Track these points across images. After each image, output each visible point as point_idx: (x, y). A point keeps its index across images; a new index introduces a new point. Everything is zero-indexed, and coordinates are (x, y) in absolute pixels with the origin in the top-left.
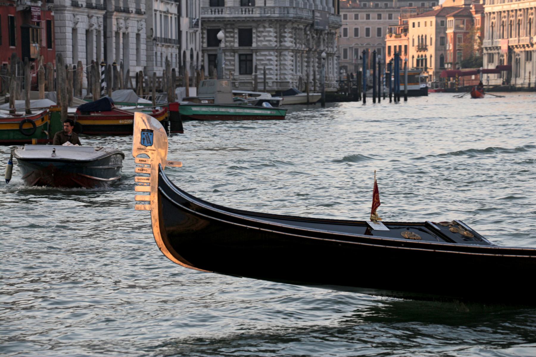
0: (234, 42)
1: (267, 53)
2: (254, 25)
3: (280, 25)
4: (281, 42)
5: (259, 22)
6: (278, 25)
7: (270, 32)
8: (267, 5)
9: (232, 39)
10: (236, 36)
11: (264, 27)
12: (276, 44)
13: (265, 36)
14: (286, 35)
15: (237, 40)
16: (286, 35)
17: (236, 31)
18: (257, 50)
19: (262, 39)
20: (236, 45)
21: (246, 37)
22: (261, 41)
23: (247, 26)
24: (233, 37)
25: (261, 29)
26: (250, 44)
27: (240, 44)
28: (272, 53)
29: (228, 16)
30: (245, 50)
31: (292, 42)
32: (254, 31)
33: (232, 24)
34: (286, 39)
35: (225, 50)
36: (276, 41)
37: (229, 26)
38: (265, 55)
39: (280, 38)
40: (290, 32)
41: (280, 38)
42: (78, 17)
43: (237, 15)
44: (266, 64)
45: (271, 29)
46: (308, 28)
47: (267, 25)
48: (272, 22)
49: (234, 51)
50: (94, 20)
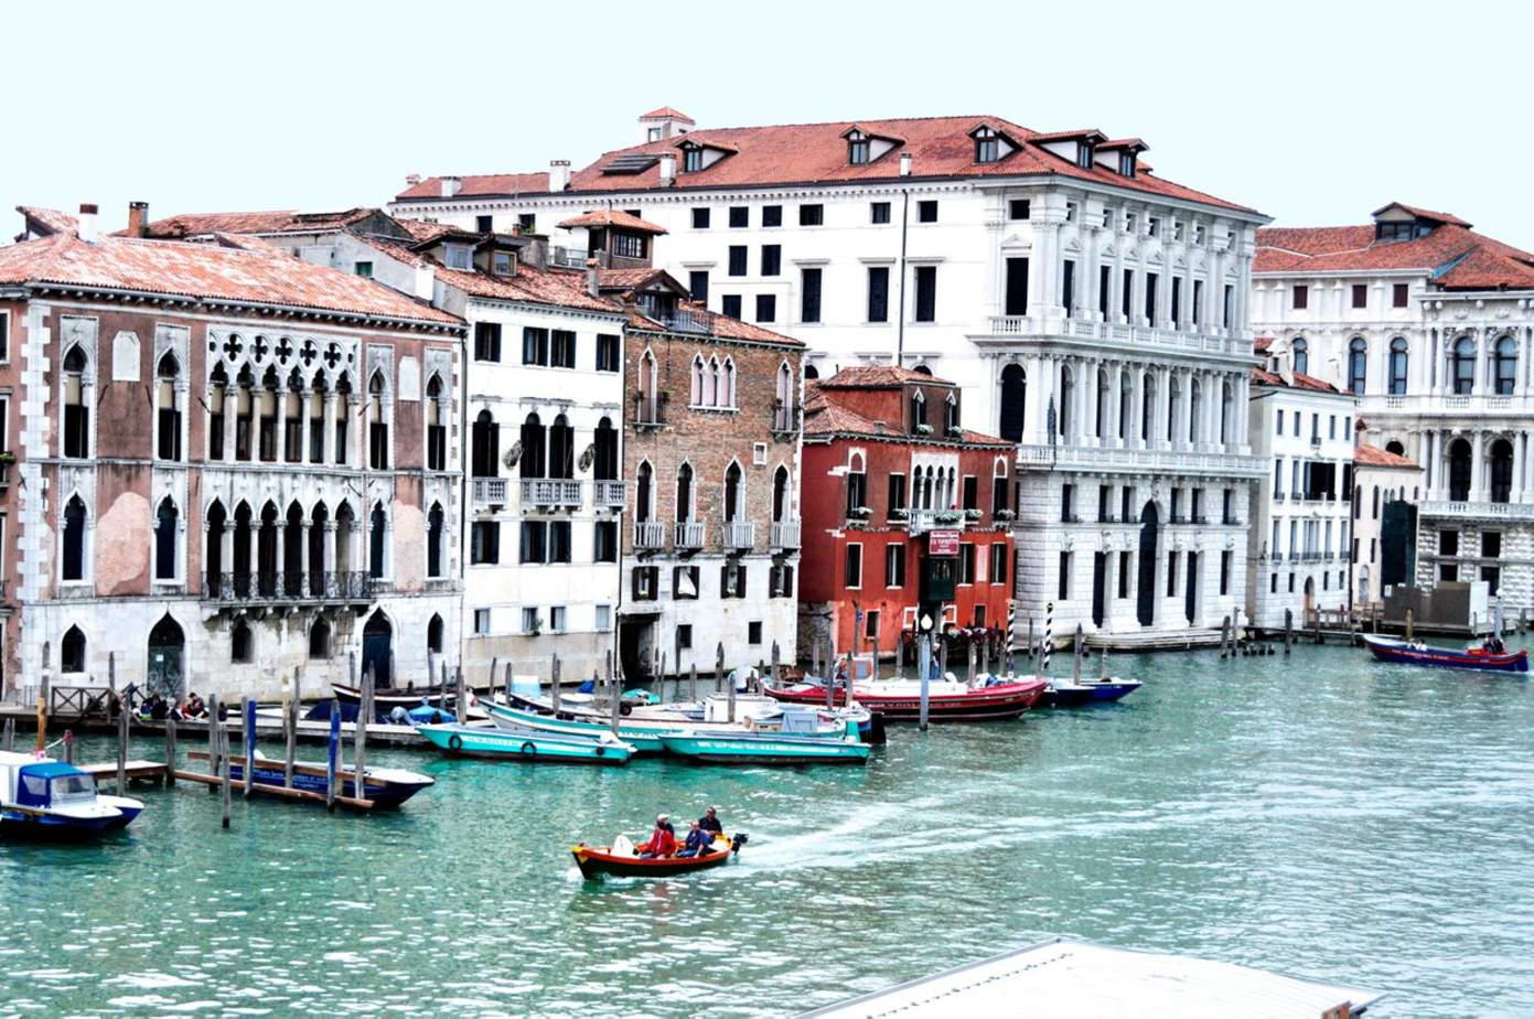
0: (1473, 549)
1: (1518, 568)
2: (1504, 528)
5: (1511, 525)
7: (1523, 539)
8: (1524, 502)
10: (1479, 542)
11: (1518, 532)
13: (1517, 545)
15: (1479, 548)
17: (1479, 535)
18: (1506, 564)
19: (1513, 547)
20: (1478, 555)
21: (1491, 545)
25: (1513, 535)
28: (1525, 568)
30: (1490, 562)
32: (1503, 536)
35: (1463, 561)
38: (1516, 571)
42: (1071, 536)
44: (1517, 584)
49: (1475, 562)
50: (1130, 537)
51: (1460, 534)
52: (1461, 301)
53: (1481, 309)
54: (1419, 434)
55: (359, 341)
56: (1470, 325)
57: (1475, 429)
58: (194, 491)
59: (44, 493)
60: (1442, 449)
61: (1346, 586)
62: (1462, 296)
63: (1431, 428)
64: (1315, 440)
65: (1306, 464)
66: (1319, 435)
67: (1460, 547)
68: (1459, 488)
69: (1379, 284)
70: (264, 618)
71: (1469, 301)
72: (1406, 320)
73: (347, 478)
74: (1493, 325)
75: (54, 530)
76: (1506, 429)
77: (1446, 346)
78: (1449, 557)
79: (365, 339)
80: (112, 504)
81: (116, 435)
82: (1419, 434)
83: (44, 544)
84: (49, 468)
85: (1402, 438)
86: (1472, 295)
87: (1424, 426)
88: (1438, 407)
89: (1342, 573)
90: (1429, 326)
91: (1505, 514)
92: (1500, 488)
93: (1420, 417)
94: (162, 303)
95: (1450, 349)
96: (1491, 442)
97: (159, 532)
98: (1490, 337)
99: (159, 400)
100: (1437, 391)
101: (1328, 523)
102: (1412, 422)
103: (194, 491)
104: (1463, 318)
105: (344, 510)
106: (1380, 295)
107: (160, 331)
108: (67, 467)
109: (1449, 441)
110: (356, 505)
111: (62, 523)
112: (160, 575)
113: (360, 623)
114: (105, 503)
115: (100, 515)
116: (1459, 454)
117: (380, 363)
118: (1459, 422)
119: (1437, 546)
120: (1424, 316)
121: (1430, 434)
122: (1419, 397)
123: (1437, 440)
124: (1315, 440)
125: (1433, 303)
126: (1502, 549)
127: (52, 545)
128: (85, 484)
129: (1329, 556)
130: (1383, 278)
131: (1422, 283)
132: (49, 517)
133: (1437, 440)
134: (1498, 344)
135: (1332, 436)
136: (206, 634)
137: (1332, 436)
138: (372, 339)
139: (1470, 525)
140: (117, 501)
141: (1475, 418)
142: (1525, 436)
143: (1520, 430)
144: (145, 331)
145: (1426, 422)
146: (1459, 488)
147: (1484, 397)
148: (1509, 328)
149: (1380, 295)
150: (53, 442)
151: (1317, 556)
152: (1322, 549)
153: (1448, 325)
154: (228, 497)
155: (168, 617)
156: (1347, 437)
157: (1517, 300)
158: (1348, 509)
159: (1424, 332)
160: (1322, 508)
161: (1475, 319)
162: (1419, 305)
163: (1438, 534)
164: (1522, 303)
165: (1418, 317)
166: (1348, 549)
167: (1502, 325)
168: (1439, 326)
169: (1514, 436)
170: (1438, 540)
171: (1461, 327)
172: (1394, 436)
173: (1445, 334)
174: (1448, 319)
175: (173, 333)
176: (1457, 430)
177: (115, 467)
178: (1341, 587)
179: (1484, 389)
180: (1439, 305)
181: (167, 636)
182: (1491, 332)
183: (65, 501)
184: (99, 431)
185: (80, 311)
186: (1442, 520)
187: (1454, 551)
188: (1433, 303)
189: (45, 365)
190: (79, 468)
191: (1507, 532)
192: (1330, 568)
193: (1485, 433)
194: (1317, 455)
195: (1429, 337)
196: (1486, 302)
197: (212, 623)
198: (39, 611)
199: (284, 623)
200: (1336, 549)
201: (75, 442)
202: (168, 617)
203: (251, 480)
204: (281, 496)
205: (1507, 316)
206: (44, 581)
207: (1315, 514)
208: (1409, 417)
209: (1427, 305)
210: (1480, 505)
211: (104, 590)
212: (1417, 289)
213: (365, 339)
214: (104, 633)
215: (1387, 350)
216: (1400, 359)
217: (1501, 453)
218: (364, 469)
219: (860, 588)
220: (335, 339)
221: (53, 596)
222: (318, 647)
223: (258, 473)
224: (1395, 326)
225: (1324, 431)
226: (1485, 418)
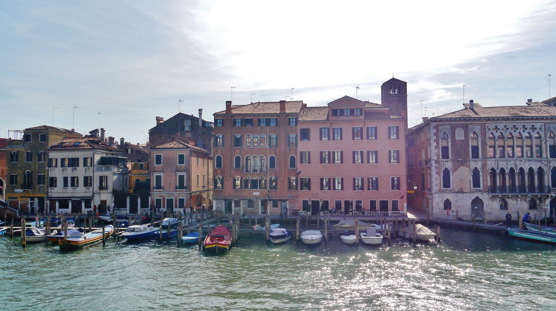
55: (543, 124)
58: (484, 166)
59: (436, 167)
70: (509, 198)
73: (541, 161)
75: (440, 176)
79: (545, 123)
80: (457, 169)
81: (457, 154)
83: (436, 179)
84: (436, 162)
94: (469, 120)
97: (473, 176)
99: (471, 143)
103: (484, 166)
105: (540, 169)
107: (470, 126)
108: (443, 161)
110: (545, 169)
111: (442, 174)
112: (474, 187)
113: (548, 201)
114: (455, 169)
115: (453, 173)
117: (552, 129)
127: (439, 180)
128: (449, 165)
132: (438, 173)
136: (491, 202)
138: (548, 123)
140: (459, 169)
144: (465, 128)
150: (438, 155)
154: (496, 166)
155: (477, 197)
175: (475, 127)
177: (458, 161)
181: (477, 202)
183: (443, 169)
184: (452, 152)
185: (445, 125)
189: (435, 138)
190: (447, 162)
197: (493, 198)
198: (436, 195)
199: (519, 199)
201: (445, 155)
202: (477, 197)
203: (504, 163)
204: (516, 166)
206: (437, 188)
211: (456, 191)
213: (545, 123)
214: (457, 201)
218: (547, 158)
219: (178, 165)
220: (533, 124)
221: (440, 191)
222: (533, 206)
223: (507, 160)
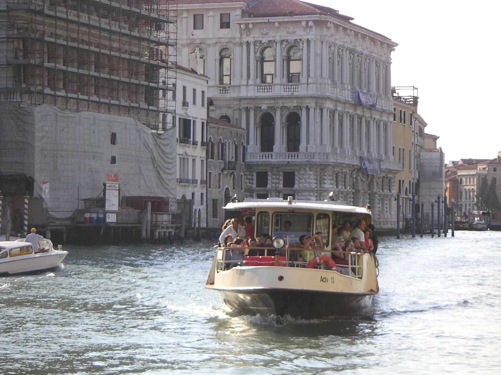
0: (279, 183)
1: (307, 194)
2: (296, 168)
3: (321, 169)
4: (321, 184)
6: (319, 169)
7: (310, 174)
9: (278, 181)
10: (281, 178)
12: (316, 185)
14: (325, 177)
15: (282, 182)
16: (325, 177)
17: (281, 173)
19: (303, 181)
20: (281, 186)
22: (302, 183)
23: (288, 169)
24: (279, 179)
25: (302, 172)
26: (292, 185)
27: (285, 186)
29: (273, 160)
31: (332, 184)
32: (296, 174)
33: (277, 168)
34: (325, 182)
36: (316, 183)
37: (275, 169)
39: (321, 181)
40: (329, 175)
41: (321, 181)
43: (281, 160)
45: (312, 173)
46: (354, 172)
47: (308, 169)
48: (311, 165)
51: (269, 173)
52: (265, 23)
53: (278, 28)
54: (240, 110)
56: (271, 39)
57: (277, 105)
60: (255, 120)
61: (205, 203)
62: (265, 20)
63: (248, 106)
64: (185, 104)
65: (180, 119)
66: (187, 100)
67: (269, 182)
68: (267, 144)
69: (211, 13)
71: (269, 23)
72: (230, 36)
74: (286, 38)
76: (295, 105)
77: (255, 53)
78: (262, 188)
82: (240, 110)
85: (229, 113)
86: (272, 19)
87: (244, 105)
88: (252, 93)
89: (202, 194)
90: (245, 39)
91: (300, 158)
92: (293, 144)
93: (241, 99)
95: (258, 55)
96: (287, 113)
98: (284, 46)
100: (251, 82)
101: (194, 160)
102: (236, 103)
104: (267, 34)
106: (212, 22)
109: (260, 114)
116: (267, 121)
118: (266, 102)
119: (255, 182)
120: (241, 34)
121: (247, 110)
122: (239, 86)
123: (252, 114)
124: (185, 104)
125: (247, 25)
126: (296, 182)
129: (194, 181)
130: (213, 9)
131: (239, 12)
133: (252, 114)
134: (288, 51)
135: (194, 103)
137: (194, 103)
139: (276, 167)
141: (274, 98)
142: (308, 109)
143: (305, 105)
145: (245, 102)
146: (267, 144)
147: (281, 85)
148: (296, 40)
149: (212, 22)
151: (188, 181)
152: (190, 177)
153: (258, 39)
156: (203, 105)
157: (301, 21)
158: (205, 151)
159: (241, 44)
160: (190, 150)
161: (274, 35)
162: (238, 26)
163: (255, 174)
164: (304, 24)
165: (238, 35)
166: (205, 179)
167: (291, 38)
168: (251, 39)
169: (301, 109)
170: (255, 178)
171: (265, 40)
172: (224, 112)
173: (255, 45)
174: (255, 35)
176: (264, 107)
178: (202, 204)
179: (281, 80)
180: (251, 26)
182: (284, 43)
186: (257, 165)
187: (265, 185)
188: (247, 25)
191: (298, 171)
192: (196, 189)
193: (283, 108)
194: (186, 113)
195: (245, 47)
196: (279, 22)
200: (198, 177)
205: (294, 32)
207: (186, 153)
208: (234, 99)
209: (242, 26)
210: (280, 155)
212: (236, 16)
215: (218, 57)
216: (226, 62)
217: (293, 120)
224: (223, 41)
225: (189, 99)
226: (282, 98)
